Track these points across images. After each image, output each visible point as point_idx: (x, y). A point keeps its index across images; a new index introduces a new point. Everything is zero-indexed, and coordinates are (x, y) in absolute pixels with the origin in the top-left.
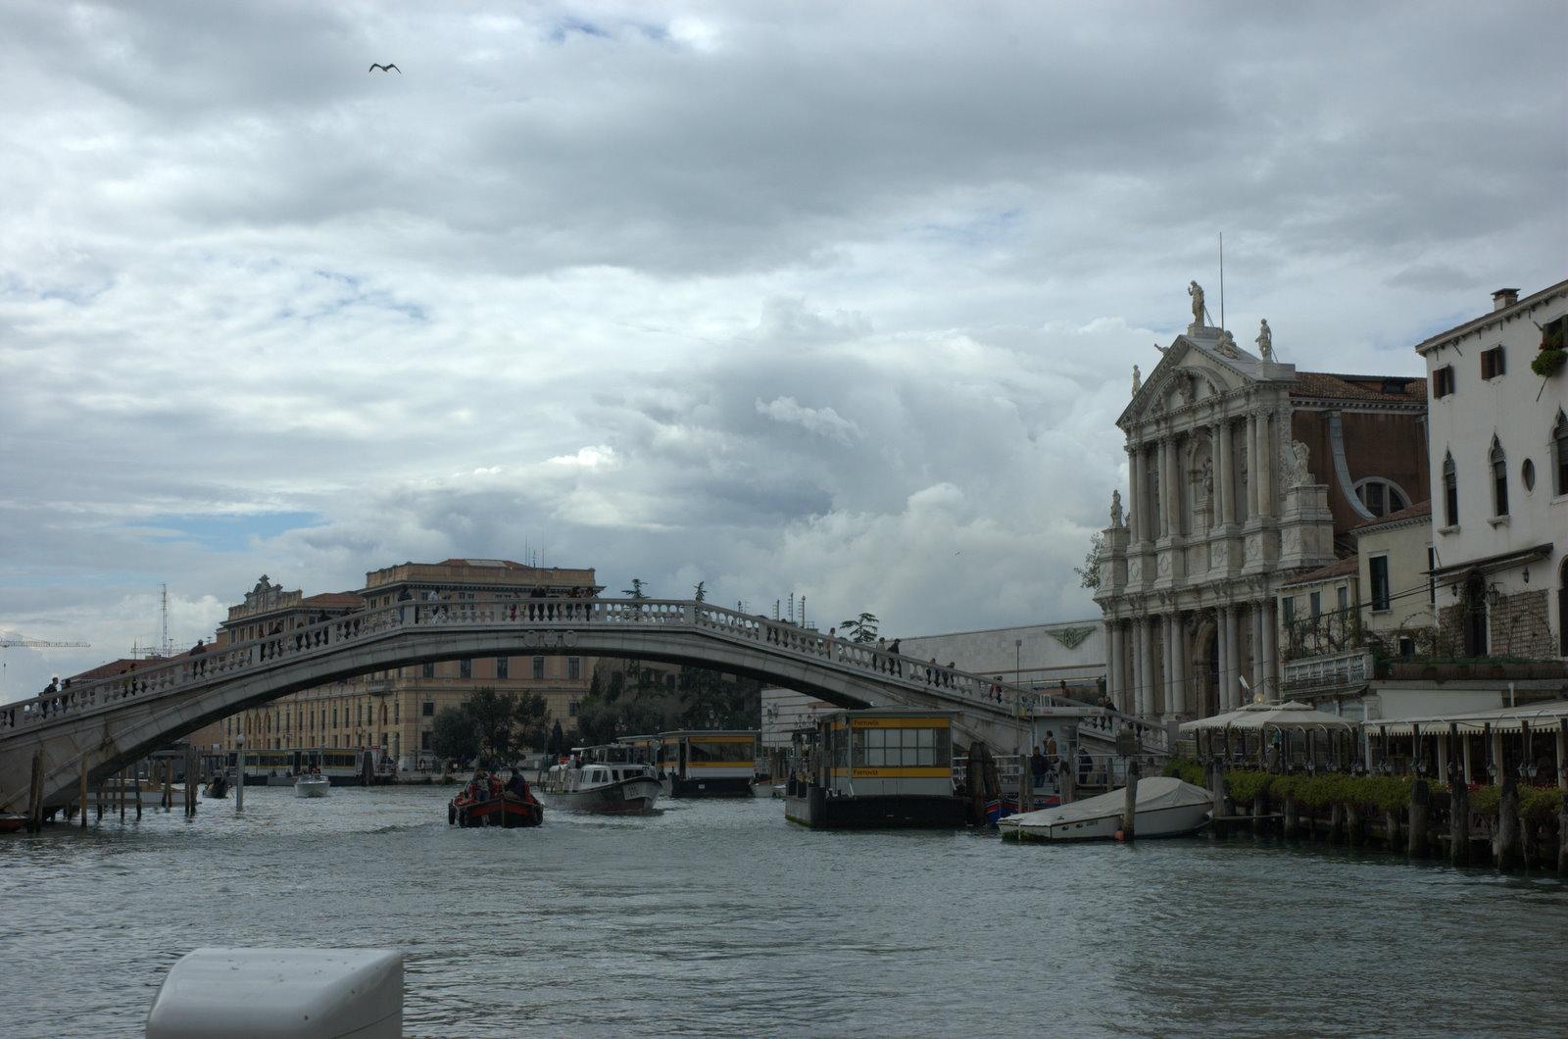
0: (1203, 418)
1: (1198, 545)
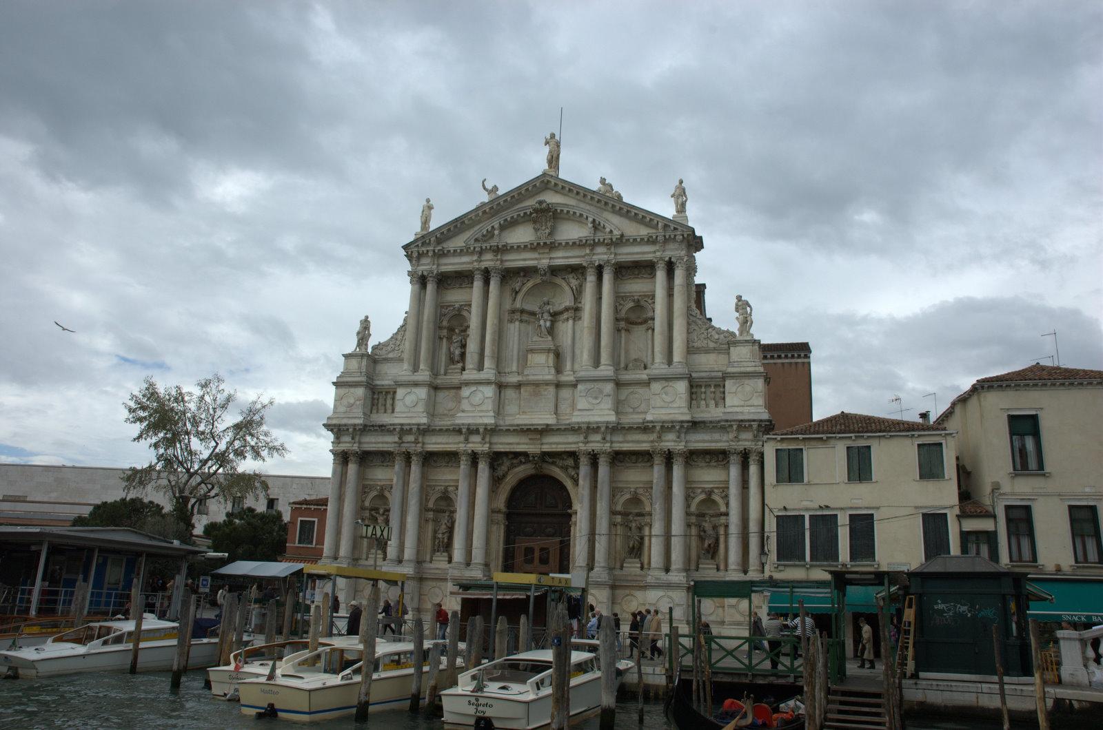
0: (561, 258)
1: (537, 384)
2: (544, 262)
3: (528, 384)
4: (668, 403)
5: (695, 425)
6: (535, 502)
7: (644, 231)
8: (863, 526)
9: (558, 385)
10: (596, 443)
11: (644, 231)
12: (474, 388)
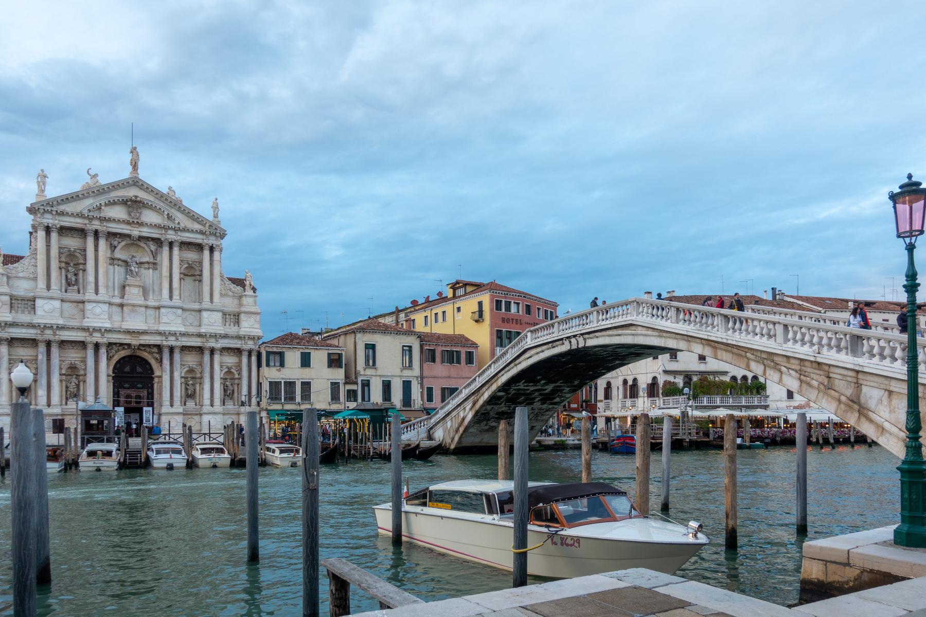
0: (146, 232)
1: (134, 306)
2: (136, 232)
3: (128, 305)
4: (212, 323)
5: (226, 336)
6: (134, 372)
7: (197, 226)
8: (306, 385)
9: (146, 307)
10: (172, 341)
11: (197, 226)
12: (94, 304)
